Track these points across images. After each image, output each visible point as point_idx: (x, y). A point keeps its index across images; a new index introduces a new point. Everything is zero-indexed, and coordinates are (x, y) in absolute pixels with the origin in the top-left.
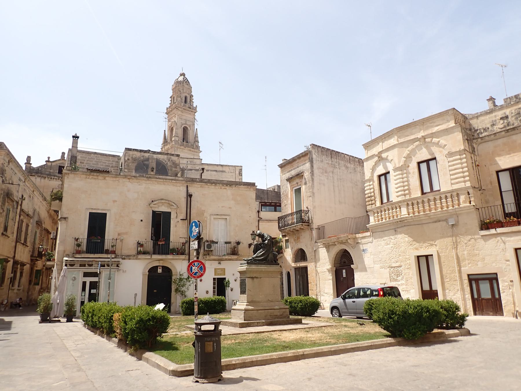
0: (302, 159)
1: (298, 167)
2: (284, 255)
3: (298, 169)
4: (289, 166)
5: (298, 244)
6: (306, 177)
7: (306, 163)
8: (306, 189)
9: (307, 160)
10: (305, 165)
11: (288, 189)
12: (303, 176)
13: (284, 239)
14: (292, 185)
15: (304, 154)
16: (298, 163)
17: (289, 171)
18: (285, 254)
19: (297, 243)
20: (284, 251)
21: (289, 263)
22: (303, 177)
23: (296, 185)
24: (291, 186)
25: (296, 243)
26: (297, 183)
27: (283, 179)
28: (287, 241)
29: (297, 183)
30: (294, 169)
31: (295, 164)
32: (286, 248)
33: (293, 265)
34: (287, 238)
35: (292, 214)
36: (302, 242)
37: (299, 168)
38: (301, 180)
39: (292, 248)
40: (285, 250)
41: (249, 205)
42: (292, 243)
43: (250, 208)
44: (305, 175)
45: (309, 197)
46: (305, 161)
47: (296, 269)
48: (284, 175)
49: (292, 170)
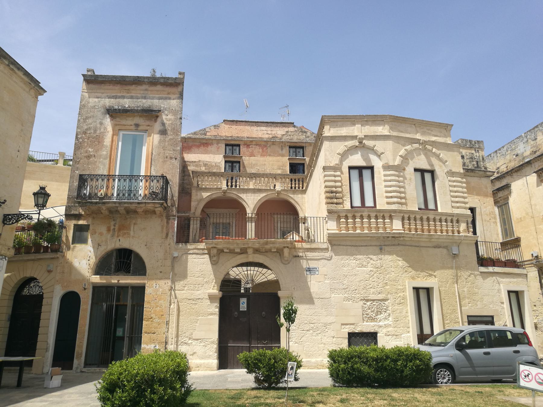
0: (159, 87)
1: (145, 98)
2: (64, 256)
3: (144, 101)
4: (117, 88)
5: (120, 238)
6: (165, 121)
7: (170, 99)
8: (160, 142)
9: (174, 94)
10: (168, 101)
11: (105, 128)
12: (157, 117)
13: (71, 224)
14: (117, 123)
15: (170, 81)
16: (146, 90)
17: (115, 97)
18: (69, 255)
19: (118, 237)
20: (69, 248)
21: (79, 273)
22: (159, 120)
23: (133, 127)
24: (114, 126)
25: (113, 236)
26: (137, 125)
27: (90, 104)
28: (79, 229)
29: (137, 125)
30: (132, 97)
31: (137, 90)
32: (73, 242)
33: (96, 279)
34: (81, 222)
35: (110, 177)
36: (133, 237)
37: (149, 100)
38: (148, 123)
39: (97, 246)
40: (72, 246)
41: (22, 125)
42: (101, 234)
43: (22, 130)
44: (164, 117)
45: (171, 158)
46: (169, 94)
47: (97, 289)
48: (96, 100)
49: (123, 97)
